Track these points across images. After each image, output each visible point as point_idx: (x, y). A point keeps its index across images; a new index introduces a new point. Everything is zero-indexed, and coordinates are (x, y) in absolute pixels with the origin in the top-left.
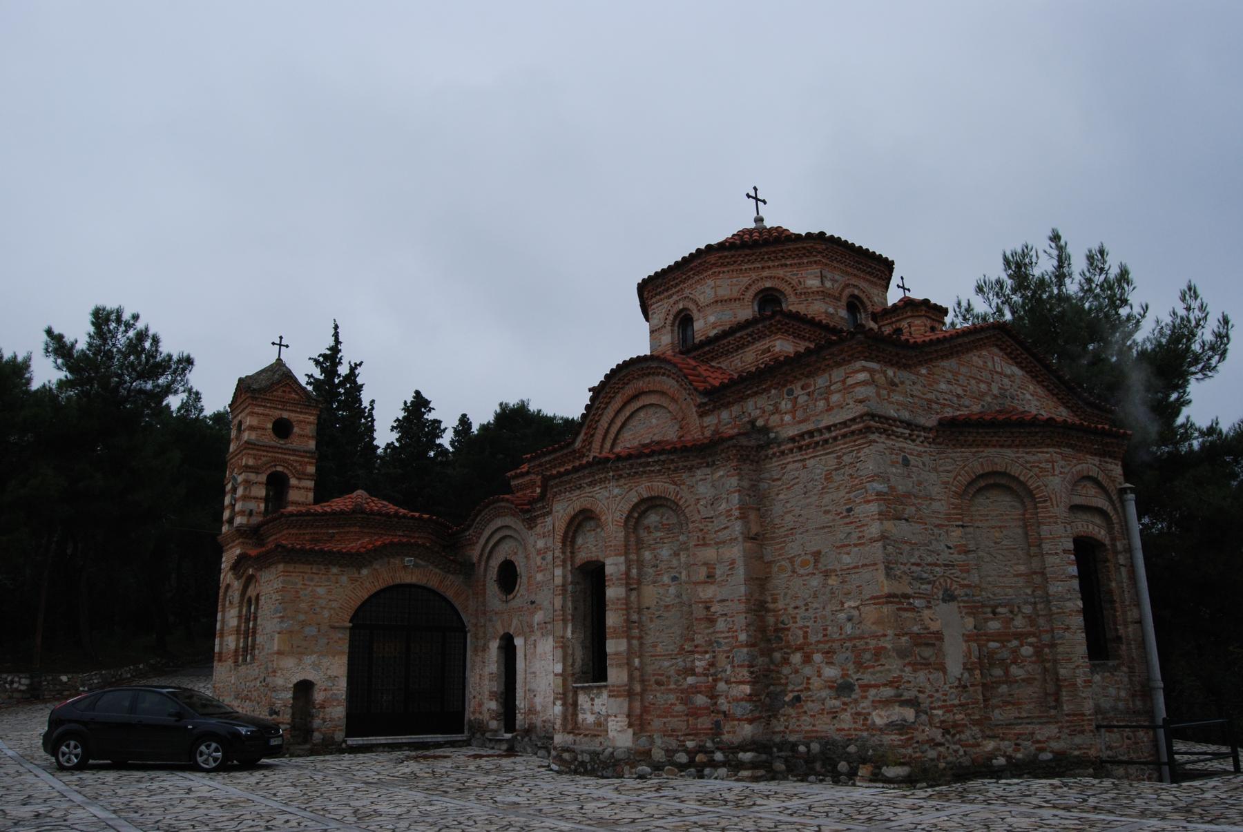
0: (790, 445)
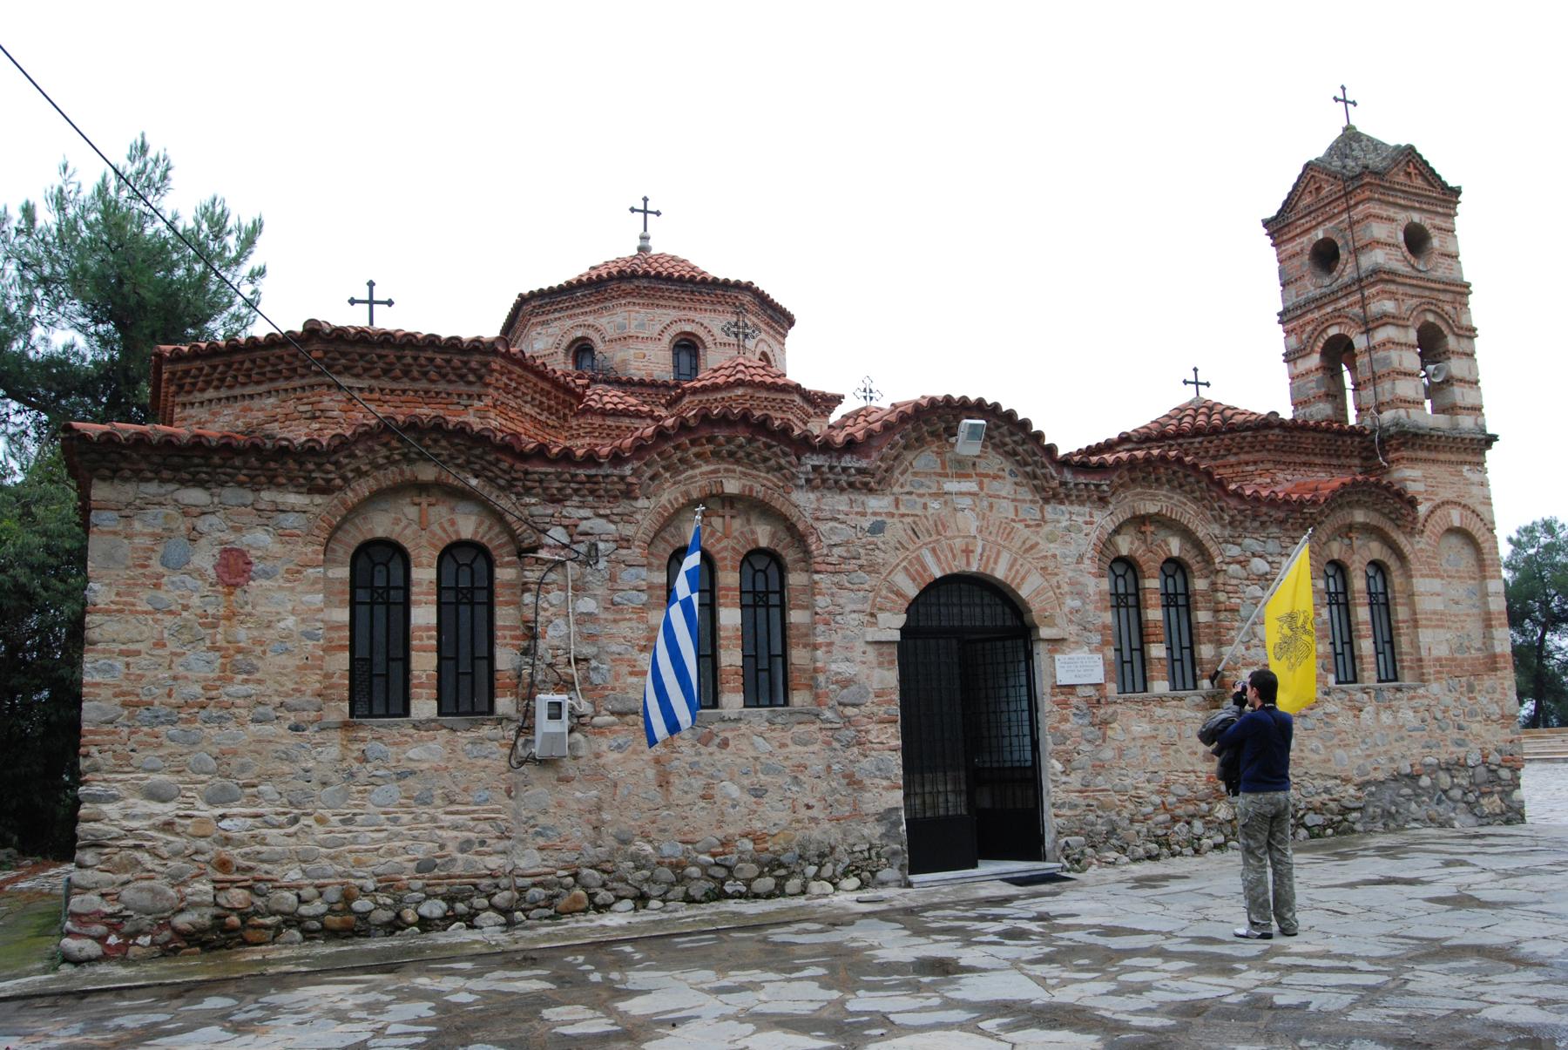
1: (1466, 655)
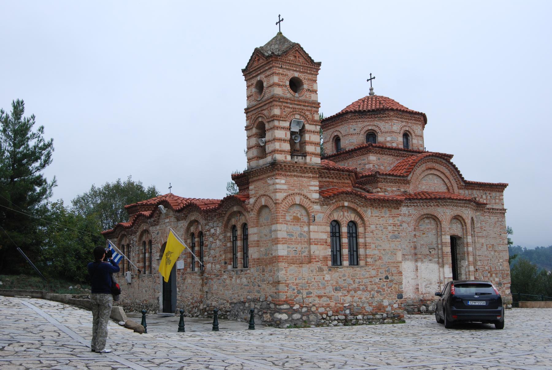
1: (268, 257)
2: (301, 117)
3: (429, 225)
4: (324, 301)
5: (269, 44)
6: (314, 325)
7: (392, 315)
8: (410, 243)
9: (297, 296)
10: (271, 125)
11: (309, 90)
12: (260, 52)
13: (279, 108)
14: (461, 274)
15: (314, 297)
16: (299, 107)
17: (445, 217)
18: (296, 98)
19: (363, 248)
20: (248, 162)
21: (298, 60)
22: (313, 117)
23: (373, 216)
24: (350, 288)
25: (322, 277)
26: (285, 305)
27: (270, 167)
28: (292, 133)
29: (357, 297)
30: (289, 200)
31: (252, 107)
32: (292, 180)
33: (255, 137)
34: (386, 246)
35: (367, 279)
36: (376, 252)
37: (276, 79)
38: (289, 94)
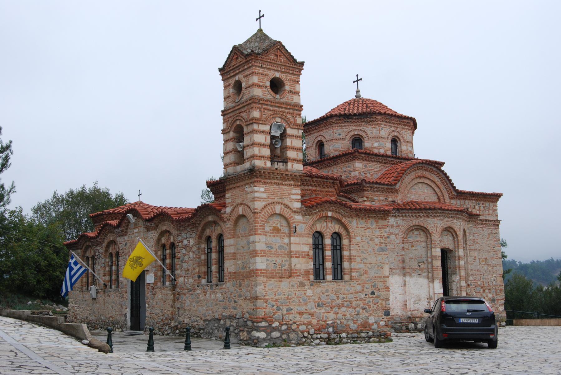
0: (480, 222)
2: (283, 121)
3: (418, 238)
4: (306, 318)
5: (248, 41)
6: (294, 344)
7: (378, 334)
8: (398, 256)
9: (276, 313)
10: (250, 128)
11: (291, 91)
12: (239, 49)
13: (258, 110)
14: (452, 290)
15: (295, 314)
16: (280, 109)
17: (435, 229)
18: (277, 100)
19: (348, 261)
20: (224, 168)
21: (280, 59)
22: (295, 120)
23: (358, 227)
24: (334, 304)
25: (303, 292)
26: (263, 323)
27: (249, 173)
28: (273, 138)
29: (341, 314)
30: (269, 209)
31: (229, 110)
32: (272, 188)
33: (232, 142)
34: (372, 259)
35: (352, 295)
36: (362, 266)
37: (255, 79)
38: (269, 95)
